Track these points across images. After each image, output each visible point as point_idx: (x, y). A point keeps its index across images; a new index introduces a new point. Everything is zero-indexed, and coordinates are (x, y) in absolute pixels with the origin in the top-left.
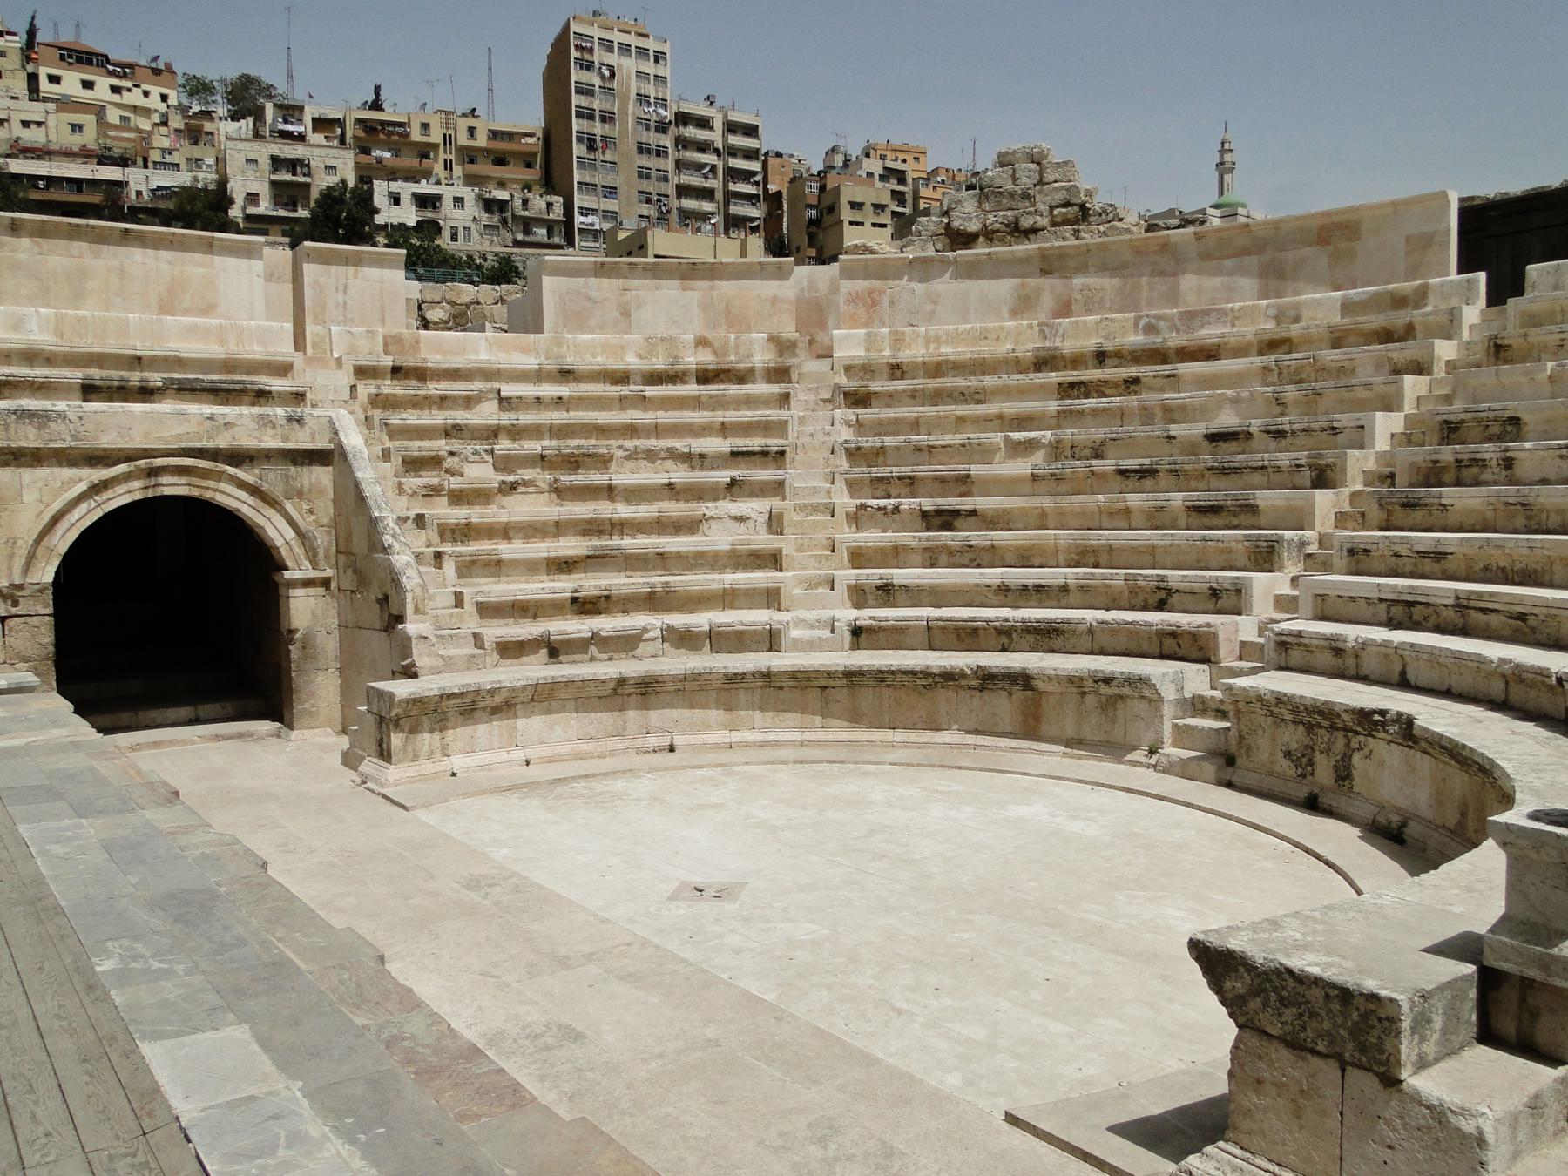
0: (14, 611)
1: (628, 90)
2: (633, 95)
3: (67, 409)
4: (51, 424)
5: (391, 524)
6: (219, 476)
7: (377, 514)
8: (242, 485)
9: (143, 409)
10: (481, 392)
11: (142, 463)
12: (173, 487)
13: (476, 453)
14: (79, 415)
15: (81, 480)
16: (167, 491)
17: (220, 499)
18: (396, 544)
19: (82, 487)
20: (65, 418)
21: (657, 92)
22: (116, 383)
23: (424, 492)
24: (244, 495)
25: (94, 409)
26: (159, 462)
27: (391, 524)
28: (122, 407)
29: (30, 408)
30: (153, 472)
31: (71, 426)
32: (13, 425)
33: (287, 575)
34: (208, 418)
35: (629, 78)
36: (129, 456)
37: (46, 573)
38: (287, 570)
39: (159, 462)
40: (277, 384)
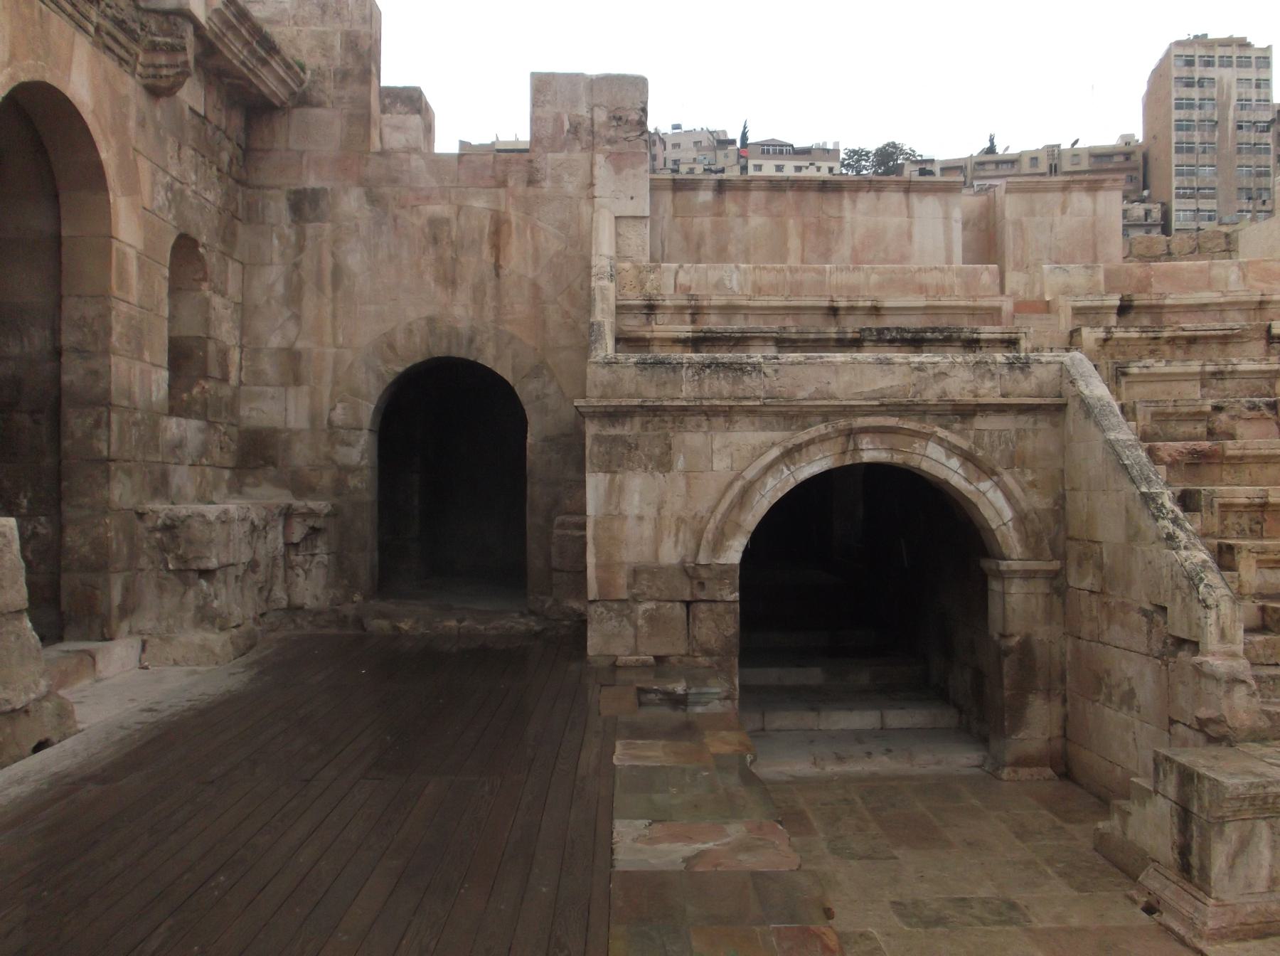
0: (703, 596)
1: (1229, 97)
2: (1234, 102)
3: (761, 360)
4: (746, 378)
5: (1169, 504)
6: (927, 437)
7: (1144, 489)
8: (952, 449)
9: (843, 359)
10: (1244, 330)
11: (842, 423)
12: (871, 452)
13: (1253, 407)
14: (776, 367)
15: (774, 444)
16: (867, 457)
17: (925, 466)
18: (1181, 535)
19: (775, 453)
20: (760, 371)
21: (1259, 94)
22: (812, 336)
23: (1187, 459)
24: (955, 463)
25: (790, 360)
26: (861, 422)
27: (1169, 504)
28: (821, 357)
29: (725, 360)
30: (851, 433)
31: (766, 380)
32: (707, 381)
33: (1004, 565)
34: (916, 368)
35: (1229, 87)
36: (827, 414)
37: (733, 554)
38: (1004, 559)
39: (861, 422)
40: (988, 331)
